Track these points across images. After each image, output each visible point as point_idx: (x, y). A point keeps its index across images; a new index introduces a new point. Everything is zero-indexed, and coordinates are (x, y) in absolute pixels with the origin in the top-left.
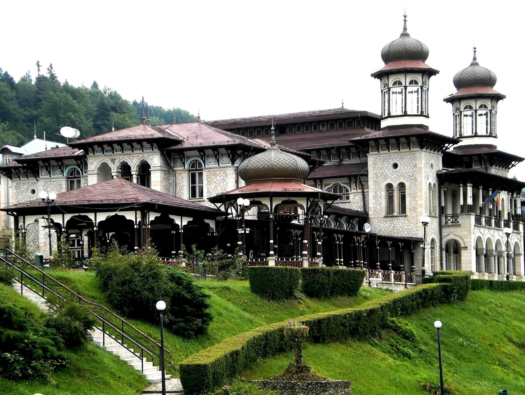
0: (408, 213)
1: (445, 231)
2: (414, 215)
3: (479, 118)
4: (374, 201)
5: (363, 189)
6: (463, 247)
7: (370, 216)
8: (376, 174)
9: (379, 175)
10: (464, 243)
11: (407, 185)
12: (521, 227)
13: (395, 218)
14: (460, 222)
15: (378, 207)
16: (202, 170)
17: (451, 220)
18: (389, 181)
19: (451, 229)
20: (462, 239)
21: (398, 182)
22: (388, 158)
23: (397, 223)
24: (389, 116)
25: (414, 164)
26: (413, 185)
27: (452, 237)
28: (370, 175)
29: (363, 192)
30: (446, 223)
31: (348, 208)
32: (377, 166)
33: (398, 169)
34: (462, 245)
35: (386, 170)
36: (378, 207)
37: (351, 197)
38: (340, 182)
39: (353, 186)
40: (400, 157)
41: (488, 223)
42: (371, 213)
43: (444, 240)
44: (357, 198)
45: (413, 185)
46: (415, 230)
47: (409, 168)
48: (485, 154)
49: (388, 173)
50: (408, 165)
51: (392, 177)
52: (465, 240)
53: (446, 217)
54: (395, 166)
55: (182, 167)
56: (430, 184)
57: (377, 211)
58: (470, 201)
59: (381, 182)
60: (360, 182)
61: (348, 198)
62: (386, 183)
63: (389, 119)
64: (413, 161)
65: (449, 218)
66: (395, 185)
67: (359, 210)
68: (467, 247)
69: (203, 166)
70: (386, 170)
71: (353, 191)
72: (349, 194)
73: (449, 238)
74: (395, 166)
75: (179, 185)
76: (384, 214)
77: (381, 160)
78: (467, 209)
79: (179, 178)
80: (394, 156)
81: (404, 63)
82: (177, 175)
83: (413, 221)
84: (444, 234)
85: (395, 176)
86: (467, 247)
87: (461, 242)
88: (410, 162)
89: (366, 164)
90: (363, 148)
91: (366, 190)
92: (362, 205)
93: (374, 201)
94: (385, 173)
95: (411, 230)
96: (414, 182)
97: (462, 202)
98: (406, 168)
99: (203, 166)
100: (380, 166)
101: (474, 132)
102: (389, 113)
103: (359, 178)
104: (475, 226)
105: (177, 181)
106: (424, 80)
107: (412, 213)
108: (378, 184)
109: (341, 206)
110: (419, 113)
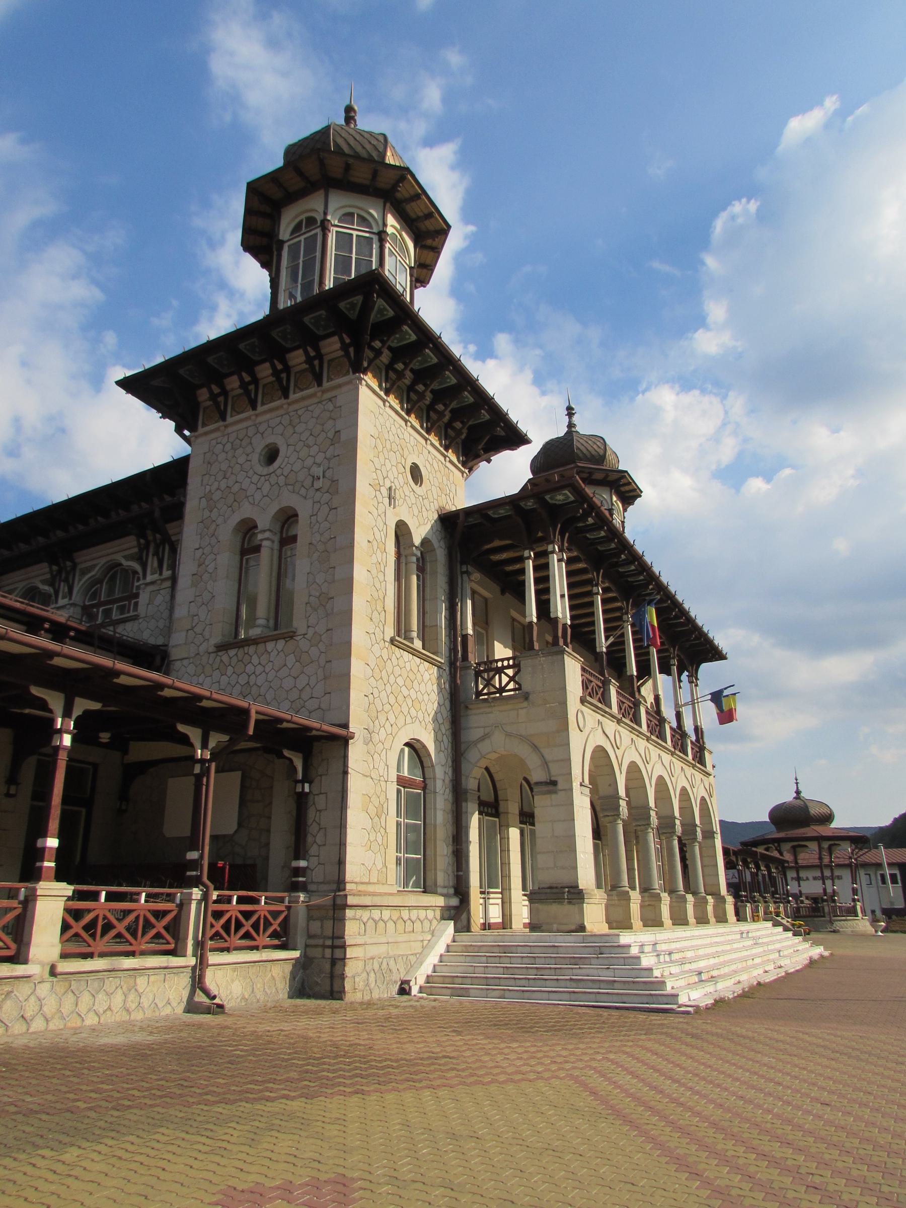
0: (299, 624)
8: (208, 497)
9: (217, 496)
10: (545, 763)
11: (304, 510)
13: (252, 649)
18: (246, 511)
20: (535, 748)
21: (274, 508)
23: (259, 669)
25: (331, 435)
37: (144, 598)
38: (119, 558)
39: (153, 562)
42: (178, 638)
45: (325, 509)
50: (311, 441)
51: (258, 496)
52: (545, 752)
54: (272, 455)
58: (562, 609)
62: (236, 518)
66: (264, 521)
68: (554, 783)
83: (314, 652)
85: (266, 488)
86: (554, 783)
94: (236, 488)
95: (305, 696)
96: (327, 497)
100: (224, 466)
104: (583, 701)
108: (213, 527)
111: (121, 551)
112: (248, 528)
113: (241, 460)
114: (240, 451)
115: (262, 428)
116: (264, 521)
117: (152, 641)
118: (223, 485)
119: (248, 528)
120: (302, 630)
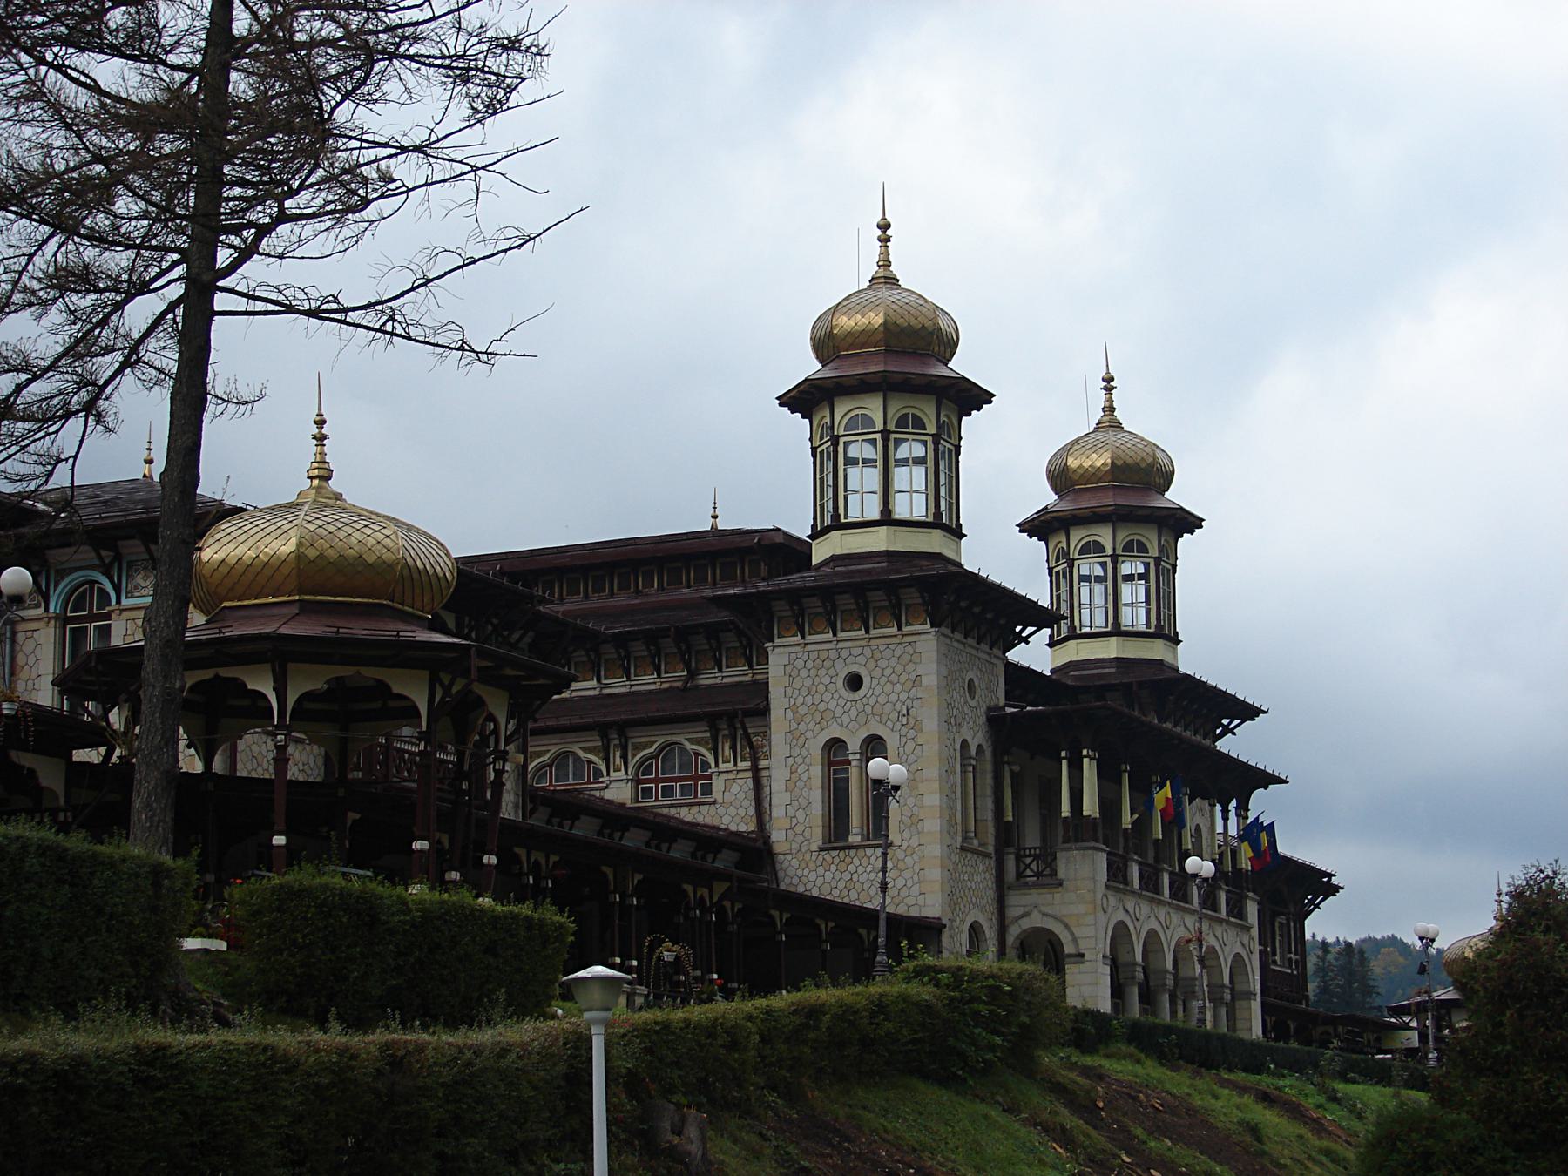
1: (1017, 902)
2: (914, 842)
3: (1125, 589)
4: (786, 798)
5: (755, 760)
6: (1070, 956)
7: (777, 848)
8: (793, 708)
9: (803, 710)
10: (1075, 940)
12: (1252, 909)
13: (853, 852)
14: (1061, 874)
15: (801, 816)
16: (108, 616)
17: (1034, 866)
19: (1033, 897)
20: (1067, 926)
21: (863, 734)
22: (833, 654)
24: (837, 525)
25: (913, 677)
26: (911, 745)
27: (1036, 921)
28: (776, 713)
29: (755, 770)
30: (1019, 875)
31: (708, 821)
32: (797, 683)
33: (862, 692)
34: (1069, 949)
35: (827, 697)
36: (801, 816)
37: (717, 784)
38: (681, 739)
40: (868, 652)
41: (1150, 883)
42: (776, 836)
43: (1014, 932)
44: (735, 788)
45: (911, 745)
46: (915, 890)
47: (898, 687)
48: (1141, 684)
49: (832, 705)
50: (894, 678)
51: (846, 719)
52: (1074, 930)
53: (1019, 859)
54: (855, 682)
55: (38, 606)
56: (964, 744)
57: (799, 829)
58: (1090, 807)
59: (809, 734)
60: (747, 737)
61: (707, 790)
62: (825, 737)
63: (835, 534)
64: (910, 667)
65: (1028, 860)
66: (854, 744)
67: (742, 828)
68: (1082, 955)
69: (113, 601)
70: (827, 697)
71: (723, 767)
72: (709, 777)
73: (1026, 924)
74: (855, 682)
75: (24, 675)
76: (817, 841)
77: (810, 664)
78: (1080, 831)
79: (28, 647)
80: (851, 648)
81: (891, 373)
82: (20, 637)
84: (1012, 912)
85: (854, 713)
86: (1082, 955)
87: (1065, 937)
88: (899, 669)
89: (761, 688)
90: (751, 627)
91: (763, 764)
92: (752, 811)
93: (786, 798)
94: (822, 707)
95: (904, 893)
97: (1065, 811)
98: (888, 688)
99: (113, 601)
100: (808, 682)
101: (1111, 620)
102: (836, 516)
103: (740, 719)
104: (1107, 887)
105: (20, 659)
106: (943, 418)
107: (906, 835)
109: (686, 815)
110: (930, 519)
111: (690, 741)
112: (835, 746)
113: (826, 680)
114: (822, 672)
115: (844, 654)
116: (854, 744)
117: (733, 828)
118: (809, 700)
119: (835, 746)
120: (897, 842)
